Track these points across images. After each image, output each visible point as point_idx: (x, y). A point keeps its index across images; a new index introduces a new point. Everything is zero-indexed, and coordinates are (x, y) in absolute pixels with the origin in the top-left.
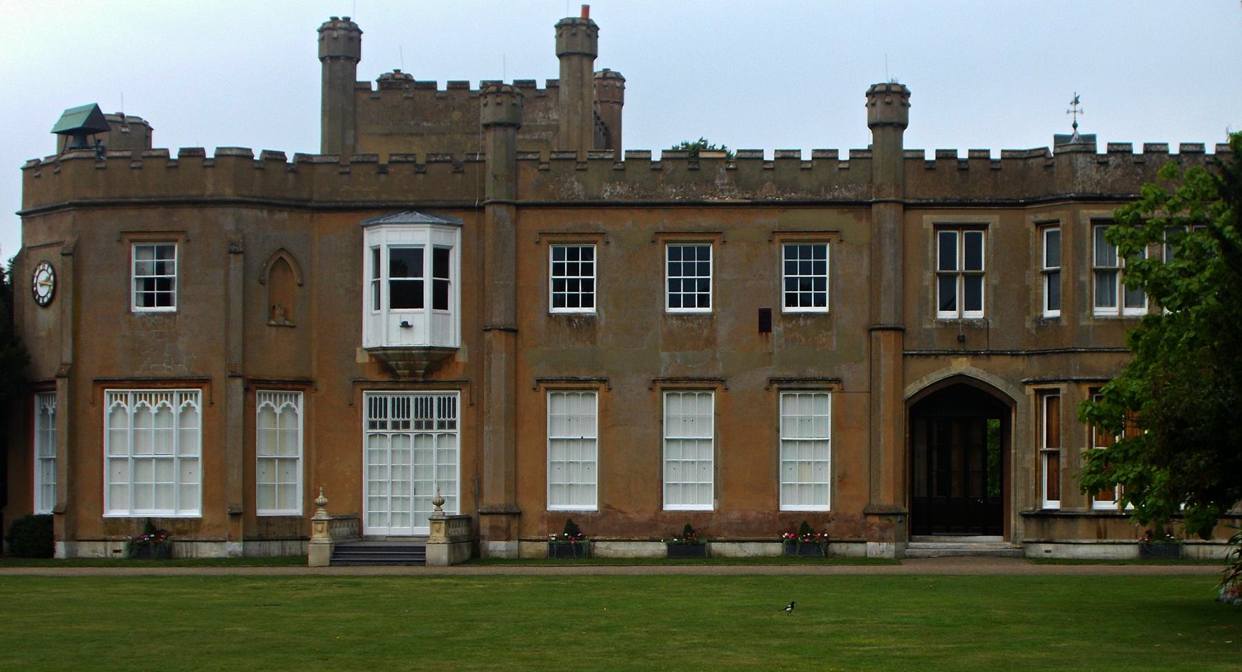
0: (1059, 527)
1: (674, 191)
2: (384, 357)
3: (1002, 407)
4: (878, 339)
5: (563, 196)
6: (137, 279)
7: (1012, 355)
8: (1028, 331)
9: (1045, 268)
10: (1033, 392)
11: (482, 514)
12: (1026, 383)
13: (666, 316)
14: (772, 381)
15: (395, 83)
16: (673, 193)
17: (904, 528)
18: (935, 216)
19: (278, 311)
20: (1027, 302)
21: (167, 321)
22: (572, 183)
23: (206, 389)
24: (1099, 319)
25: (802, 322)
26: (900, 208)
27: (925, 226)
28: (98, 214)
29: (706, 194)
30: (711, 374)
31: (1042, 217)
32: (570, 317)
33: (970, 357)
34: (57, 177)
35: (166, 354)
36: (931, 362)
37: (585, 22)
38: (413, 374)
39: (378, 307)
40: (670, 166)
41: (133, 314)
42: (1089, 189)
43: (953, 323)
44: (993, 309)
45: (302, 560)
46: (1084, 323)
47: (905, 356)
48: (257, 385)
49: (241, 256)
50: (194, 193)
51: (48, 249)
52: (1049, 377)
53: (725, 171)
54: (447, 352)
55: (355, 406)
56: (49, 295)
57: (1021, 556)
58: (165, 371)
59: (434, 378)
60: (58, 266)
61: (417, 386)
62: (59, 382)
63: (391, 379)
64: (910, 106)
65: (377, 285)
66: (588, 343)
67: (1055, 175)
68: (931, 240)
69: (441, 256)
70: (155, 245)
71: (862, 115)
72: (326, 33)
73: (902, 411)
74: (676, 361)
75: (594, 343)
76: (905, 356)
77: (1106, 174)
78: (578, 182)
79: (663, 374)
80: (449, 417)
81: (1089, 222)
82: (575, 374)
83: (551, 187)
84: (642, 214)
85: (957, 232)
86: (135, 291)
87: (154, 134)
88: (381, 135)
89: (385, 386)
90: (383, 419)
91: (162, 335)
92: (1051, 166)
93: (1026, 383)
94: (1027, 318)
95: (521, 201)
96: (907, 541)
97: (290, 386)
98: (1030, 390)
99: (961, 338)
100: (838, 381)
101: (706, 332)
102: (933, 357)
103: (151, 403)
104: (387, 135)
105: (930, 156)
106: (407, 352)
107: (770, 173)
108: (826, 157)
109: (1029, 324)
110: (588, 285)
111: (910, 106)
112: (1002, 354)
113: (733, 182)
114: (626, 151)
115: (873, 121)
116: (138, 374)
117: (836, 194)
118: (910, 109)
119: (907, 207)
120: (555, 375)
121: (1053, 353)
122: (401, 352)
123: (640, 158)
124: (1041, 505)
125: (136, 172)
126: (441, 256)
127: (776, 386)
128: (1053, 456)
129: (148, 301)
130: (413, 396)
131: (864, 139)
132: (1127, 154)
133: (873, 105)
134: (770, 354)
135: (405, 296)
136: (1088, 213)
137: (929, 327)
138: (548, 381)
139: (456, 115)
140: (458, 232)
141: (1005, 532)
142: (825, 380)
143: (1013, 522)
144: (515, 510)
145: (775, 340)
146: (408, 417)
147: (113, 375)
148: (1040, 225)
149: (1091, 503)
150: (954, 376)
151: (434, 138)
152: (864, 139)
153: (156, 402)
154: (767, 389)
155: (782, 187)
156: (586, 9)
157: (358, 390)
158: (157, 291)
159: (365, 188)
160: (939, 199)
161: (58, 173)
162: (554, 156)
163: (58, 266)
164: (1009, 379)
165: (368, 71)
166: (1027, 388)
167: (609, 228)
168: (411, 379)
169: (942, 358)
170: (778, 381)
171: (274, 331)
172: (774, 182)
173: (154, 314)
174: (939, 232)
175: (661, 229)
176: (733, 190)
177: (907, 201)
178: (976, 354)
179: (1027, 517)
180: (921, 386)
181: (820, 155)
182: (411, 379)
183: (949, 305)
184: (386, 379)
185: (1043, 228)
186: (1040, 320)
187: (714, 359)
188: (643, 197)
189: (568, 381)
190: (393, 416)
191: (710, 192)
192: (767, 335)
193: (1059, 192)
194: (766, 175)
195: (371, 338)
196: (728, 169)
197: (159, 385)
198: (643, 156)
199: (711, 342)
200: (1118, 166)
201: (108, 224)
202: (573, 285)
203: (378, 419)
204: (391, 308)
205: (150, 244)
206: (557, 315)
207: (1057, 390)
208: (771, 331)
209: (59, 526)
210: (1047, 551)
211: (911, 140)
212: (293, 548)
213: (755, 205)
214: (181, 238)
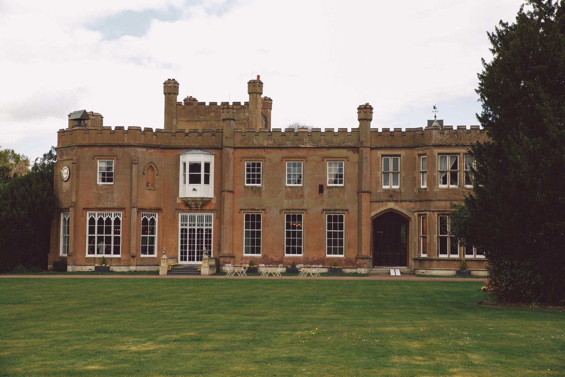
0: (427, 264)
1: (289, 143)
2: (187, 201)
4: (361, 196)
5: (250, 144)
6: (99, 172)
7: (409, 201)
8: (415, 193)
9: (421, 170)
10: (417, 215)
11: (221, 257)
12: (415, 212)
13: (286, 187)
14: (323, 210)
15: (190, 101)
16: (289, 144)
17: (370, 263)
18: (382, 152)
19: (150, 184)
20: (415, 182)
21: (110, 187)
22: (254, 140)
23: (123, 212)
24: (440, 189)
25: (334, 189)
26: (370, 148)
27: (378, 156)
28: (86, 149)
29: (300, 144)
30: (302, 208)
31: (420, 152)
32: (252, 187)
33: (394, 202)
34: (71, 135)
35: (109, 199)
36: (380, 204)
37: (258, 81)
38: (197, 207)
40: (288, 134)
41: (98, 185)
42: (437, 142)
43: (388, 190)
44: (403, 185)
45: (157, 273)
46: (435, 190)
47: (371, 202)
48: (142, 211)
49: (137, 165)
50: (120, 142)
51: (67, 161)
52: (423, 210)
53: (307, 136)
54: (209, 199)
55: (175, 218)
56: (67, 178)
57: (413, 273)
58: (109, 205)
59: (204, 208)
60: (71, 167)
61: (198, 211)
62: (71, 209)
63: (189, 209)
64: (373, 113)
65: (185, 175)
66: (258, 197)
67: (425, 137)
68: (380, 160)
69: (207, 165)
70: (106, 160)
71: (356, 116)
72: (166, 84)
73: (370, 221)
74: (290, 203)
75: (260, 195)
76: (371, 202)
77: (443, 137)
78: (255, 139)
79: (285, 207)
80: (209, 222)
81: (437, 154)
82: (254, 207)
83: (246, 141)
84: (278, 151)
85: (390, 157)
86: (99, 176)
87: (104, 120)
88: (186, 121)
89: (187, 211)
90: (186, 223)
92: (424, 134)
93: (415, 212)
94: (415, 188)
95: (236, 146)
96: (372, 268)
97: (153, 211)
98: (416, 214)
99: (391, 195)
100: (347, 210)
101: (300, 193)
102: (381, 202)
103: (104, 216)
104: (188, 121)
105: (380, 130)
106: (195, 199)
107: (323, 136)
108: (343, 131)
109: (416, 191)
110: (259, 176)
111: (373, 113)
112: (406, 201)
113: (310, 140)
114: (273, 129)
115: (360, 118)
116: (99, 206)
117: (346, 144)
118: (373, 114)
119: (372, 149)
120: (247, 208)
121: (424, 201)
122: (193, 199)
123: (277, 131)
124: (420, 256)
125: (99, 134)
126: (207, 165)
127: (325, 212)
128: (424, 238)
129: (103, 180)
130: (196, 215)
131: (357, 125)
132: (451, 130)
133: (360, 112)
134: (323, 201)
135: (195, 180)
136: (436, 151)
137: (380, 191)
138: (244, 210)
139: (212, 114)
140: (213, 156)
141: (407, 266)
142: (342, 210)
143: (410, 262)
144: (232, 256)
145: (325, 196)
146: (195, 222)
147: (90, 206)
148: (420, 155)
149: (438, 255)
150: (389, 209)
151: (204, 123)
152: (357, 125)
153: (106, 216)
154: (322, 213)
155: (327, 142)
156: (258, 77)
157: (177, 212)
158: (108, 176)
159: (180, 141)
160: (383, 146)
161: (71, 134)
162: (247, 130)
163: (71, 167)
164: (408, 210)
165: (180, 98)
166: (415, 213)
167: (266, 156)
168: (196, 209)
169: (384, 202)
170: (326, 210)
171: (148, 191)
172: (325, 140)
173: (105, 185)
174: (383, 157)
175: (285, 156)
176: (310, 143)
177: (372, 147)
178: (396, 201)
179: (415, 260)
180: (377, 212)
181: (341, 130)
182: (196, 209)
183: (386, 183)
184: (187, 208)
185: (421, 156)
186: (420, 189)
187: (303, 202)
188: (278, 145)
189: (251, 210)
190: (190, 222)
191: (302, 143)
192: (322, 194)
193: (426, 143)
194: (322, 137)
195: (181, 195)
196: (308, 135)
197: (107, 210)
198: (279, 130)
199: (302, 196)
200: (448, 134)
201: (88, 152)
202: (254, 176)
203: (184, 223)
204: (190, 183)
205: (104, 160)
206: (248, 187)
207: (426, 214)
208: (323, 193)
209: (69, 261)
210: (422, 272)
211: (373, 125)
212: (154, 268)
213: (318, 148)
214: (115, 158)
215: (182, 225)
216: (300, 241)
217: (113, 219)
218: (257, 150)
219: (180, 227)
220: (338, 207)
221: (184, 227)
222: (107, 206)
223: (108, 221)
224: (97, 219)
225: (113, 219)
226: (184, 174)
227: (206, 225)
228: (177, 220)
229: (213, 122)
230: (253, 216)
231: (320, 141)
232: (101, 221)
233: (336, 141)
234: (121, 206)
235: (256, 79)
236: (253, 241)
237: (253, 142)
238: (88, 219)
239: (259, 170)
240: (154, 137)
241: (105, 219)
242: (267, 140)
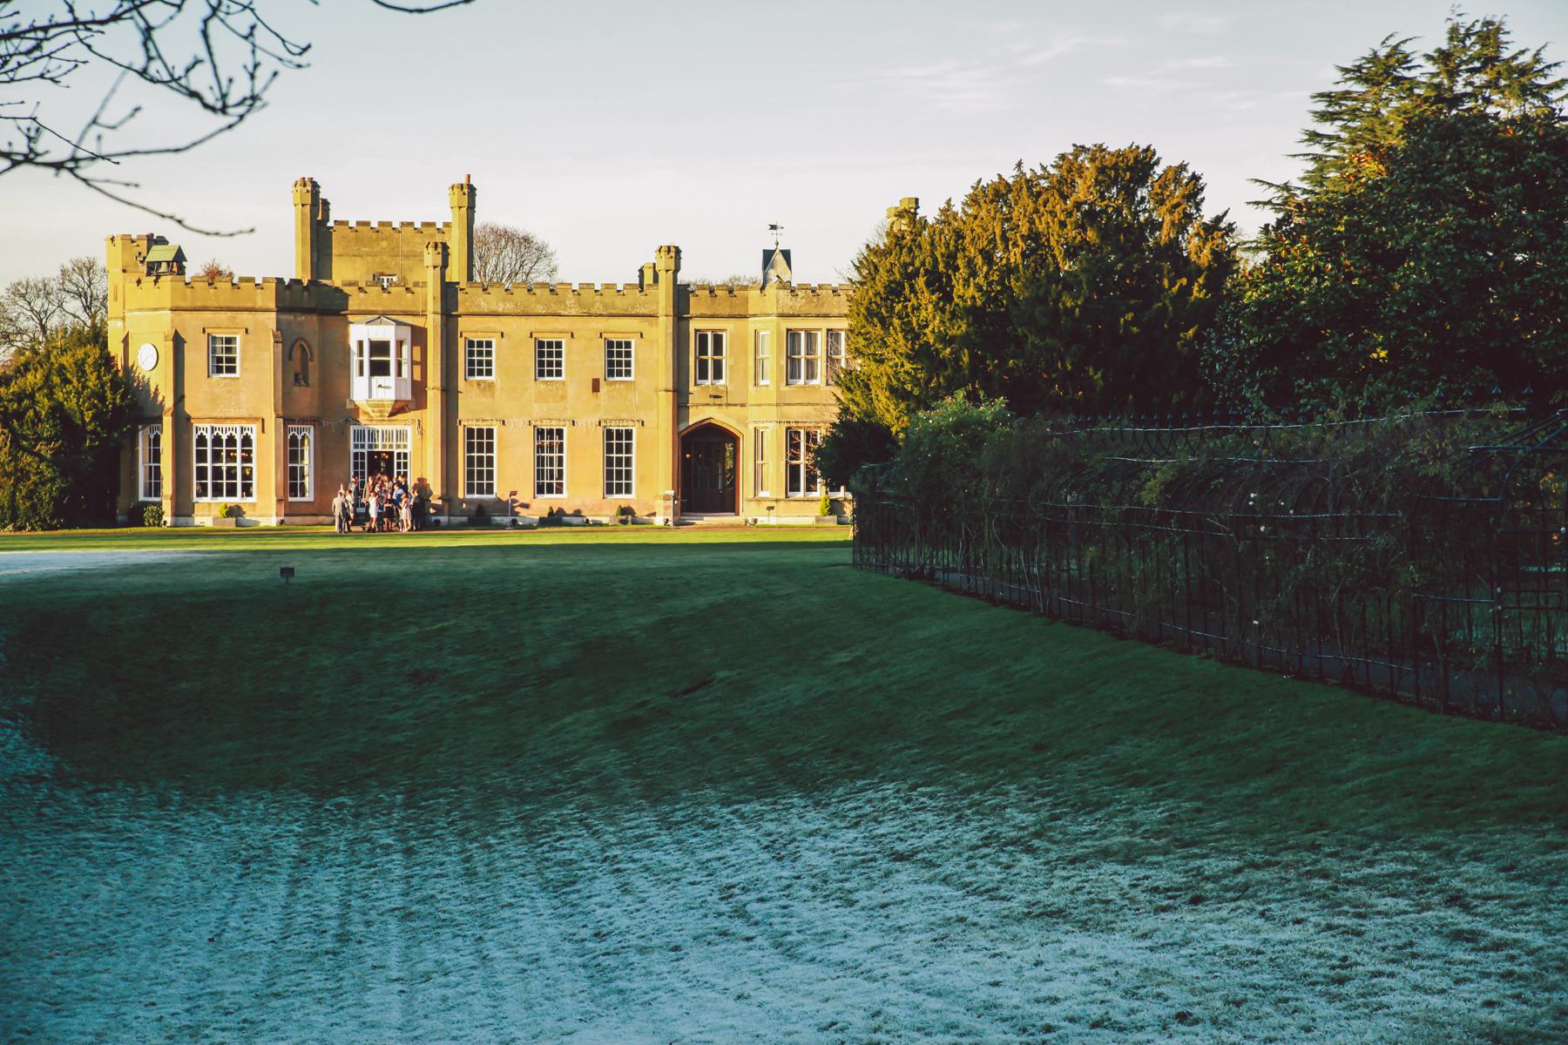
3: (734, 439)
5: (476, 310)
16: (540, 309)
32: (479, 384)
39: (361, 374)
50: (249, 305)
58: (232, 414)
75: (493, 396)
91: (230, 391)
110: (489, 363)
116: (214, 415)
126: (400, 344)
135: (379, 369)
139: (384, 244)
151: (370, 259)
155: (605, 306)
187: (565, 408)
199: (563, 398)
215: (356, 446)
216: (628, 474)
217: (238, 438)
218: (486, 318)
219: (353, 450)
220: (624, 416)
221: (360, 450)
222: (228, 415)
223: (231, 441)
224: (209, 438)
225: (238, 438)
226: (359, 360)
227: (398, 447)
228: (348, 436)
229: (385, 258)
230: (480, 431)
231: (593, 305)
232: (217, 441)
233: (621, 304)
234: (255, 415)
235: (464, 181)
236: (480, 476)
237: (479, 305)
238: (195, 437)
239: (489, 353)
240: (306, 294)
241: (224, 437)
242: (504, 300)
